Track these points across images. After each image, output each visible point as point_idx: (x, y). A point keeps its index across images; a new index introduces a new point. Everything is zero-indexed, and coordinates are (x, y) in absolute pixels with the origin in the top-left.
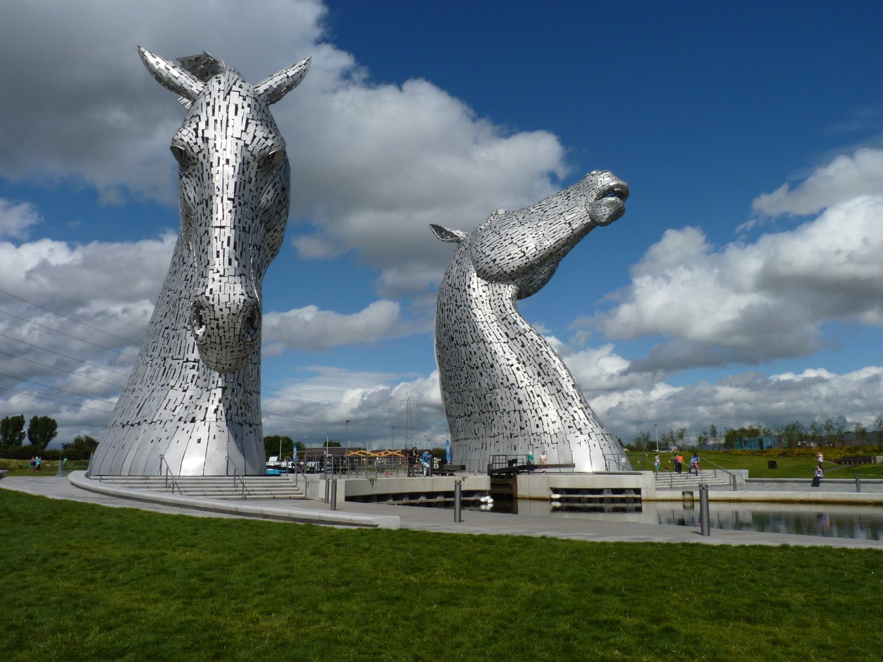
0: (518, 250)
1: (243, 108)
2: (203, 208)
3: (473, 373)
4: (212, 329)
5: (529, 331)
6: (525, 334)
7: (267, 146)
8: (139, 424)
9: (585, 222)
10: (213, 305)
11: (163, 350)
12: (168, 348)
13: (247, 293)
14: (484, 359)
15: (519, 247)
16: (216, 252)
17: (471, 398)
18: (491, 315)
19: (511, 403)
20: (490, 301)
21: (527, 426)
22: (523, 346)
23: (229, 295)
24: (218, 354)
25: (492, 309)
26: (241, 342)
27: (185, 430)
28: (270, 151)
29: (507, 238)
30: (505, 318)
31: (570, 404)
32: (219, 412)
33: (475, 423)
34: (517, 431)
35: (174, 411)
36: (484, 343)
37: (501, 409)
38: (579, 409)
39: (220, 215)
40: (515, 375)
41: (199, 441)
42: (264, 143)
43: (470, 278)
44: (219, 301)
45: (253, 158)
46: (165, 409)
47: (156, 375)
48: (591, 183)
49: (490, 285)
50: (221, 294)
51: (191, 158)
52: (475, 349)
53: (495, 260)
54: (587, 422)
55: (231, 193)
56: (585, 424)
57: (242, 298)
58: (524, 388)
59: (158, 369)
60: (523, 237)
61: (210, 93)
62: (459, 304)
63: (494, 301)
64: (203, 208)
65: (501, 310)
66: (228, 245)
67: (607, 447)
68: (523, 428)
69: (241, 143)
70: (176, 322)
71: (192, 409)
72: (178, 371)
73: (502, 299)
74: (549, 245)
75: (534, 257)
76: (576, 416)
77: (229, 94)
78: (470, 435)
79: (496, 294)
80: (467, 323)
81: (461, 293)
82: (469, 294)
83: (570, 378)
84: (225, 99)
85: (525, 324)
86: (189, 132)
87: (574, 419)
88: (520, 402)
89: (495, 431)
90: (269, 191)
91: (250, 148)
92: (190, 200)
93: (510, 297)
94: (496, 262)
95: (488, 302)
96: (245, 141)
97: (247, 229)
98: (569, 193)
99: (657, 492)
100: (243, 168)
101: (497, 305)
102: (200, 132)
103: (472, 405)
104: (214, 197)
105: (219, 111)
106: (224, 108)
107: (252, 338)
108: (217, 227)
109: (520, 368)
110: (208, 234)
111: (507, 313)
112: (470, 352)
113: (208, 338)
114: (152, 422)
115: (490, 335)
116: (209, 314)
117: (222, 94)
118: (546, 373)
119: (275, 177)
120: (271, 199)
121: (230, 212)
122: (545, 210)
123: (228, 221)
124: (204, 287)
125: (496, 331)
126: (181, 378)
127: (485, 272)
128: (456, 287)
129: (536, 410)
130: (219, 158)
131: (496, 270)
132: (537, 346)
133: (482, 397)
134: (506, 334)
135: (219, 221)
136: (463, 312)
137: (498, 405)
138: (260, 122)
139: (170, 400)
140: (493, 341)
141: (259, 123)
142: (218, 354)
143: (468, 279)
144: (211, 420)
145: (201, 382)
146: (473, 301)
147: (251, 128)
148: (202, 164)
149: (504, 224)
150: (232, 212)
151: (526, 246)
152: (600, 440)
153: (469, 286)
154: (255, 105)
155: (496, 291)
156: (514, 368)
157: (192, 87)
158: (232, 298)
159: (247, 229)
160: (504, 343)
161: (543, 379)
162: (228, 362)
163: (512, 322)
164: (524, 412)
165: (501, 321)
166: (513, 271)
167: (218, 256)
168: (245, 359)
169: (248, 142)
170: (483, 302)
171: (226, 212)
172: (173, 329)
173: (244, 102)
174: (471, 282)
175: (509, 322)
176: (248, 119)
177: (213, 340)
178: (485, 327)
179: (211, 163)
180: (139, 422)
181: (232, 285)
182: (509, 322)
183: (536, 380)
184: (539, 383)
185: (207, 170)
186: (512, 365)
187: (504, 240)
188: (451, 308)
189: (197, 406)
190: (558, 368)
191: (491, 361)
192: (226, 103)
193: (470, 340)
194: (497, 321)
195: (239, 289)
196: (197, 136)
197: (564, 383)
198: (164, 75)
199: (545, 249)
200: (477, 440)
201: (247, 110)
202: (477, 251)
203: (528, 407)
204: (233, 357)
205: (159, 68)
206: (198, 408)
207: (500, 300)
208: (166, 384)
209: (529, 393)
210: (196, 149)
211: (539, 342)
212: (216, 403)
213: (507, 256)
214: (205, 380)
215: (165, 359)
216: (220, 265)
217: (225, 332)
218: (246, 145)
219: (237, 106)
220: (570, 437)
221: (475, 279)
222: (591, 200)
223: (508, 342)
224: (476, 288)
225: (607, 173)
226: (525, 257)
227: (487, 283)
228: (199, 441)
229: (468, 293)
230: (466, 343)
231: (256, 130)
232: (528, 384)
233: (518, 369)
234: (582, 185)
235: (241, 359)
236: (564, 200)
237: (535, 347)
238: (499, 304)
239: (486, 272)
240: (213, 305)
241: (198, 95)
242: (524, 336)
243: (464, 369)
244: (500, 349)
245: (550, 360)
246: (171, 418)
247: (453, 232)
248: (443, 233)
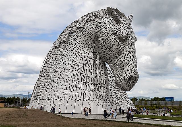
2: (128, 53)
8: (86, 100)
11: (83, 80)
12: (85, 79)
31: (124, 95)
35: (97, 97)
59: (83, 85)
64: (128, 53)
70: (86, 72)
72: (92, 87)
87: (126, 99)
110: (133, 60)
114: (92, 100)
148: (128, 43)
164: (113, 96)
172: (85, 74)
179: (131, 43)
185: (130, 45)
208: (89, 90)
210: (127, 39)
214: (102, 90)
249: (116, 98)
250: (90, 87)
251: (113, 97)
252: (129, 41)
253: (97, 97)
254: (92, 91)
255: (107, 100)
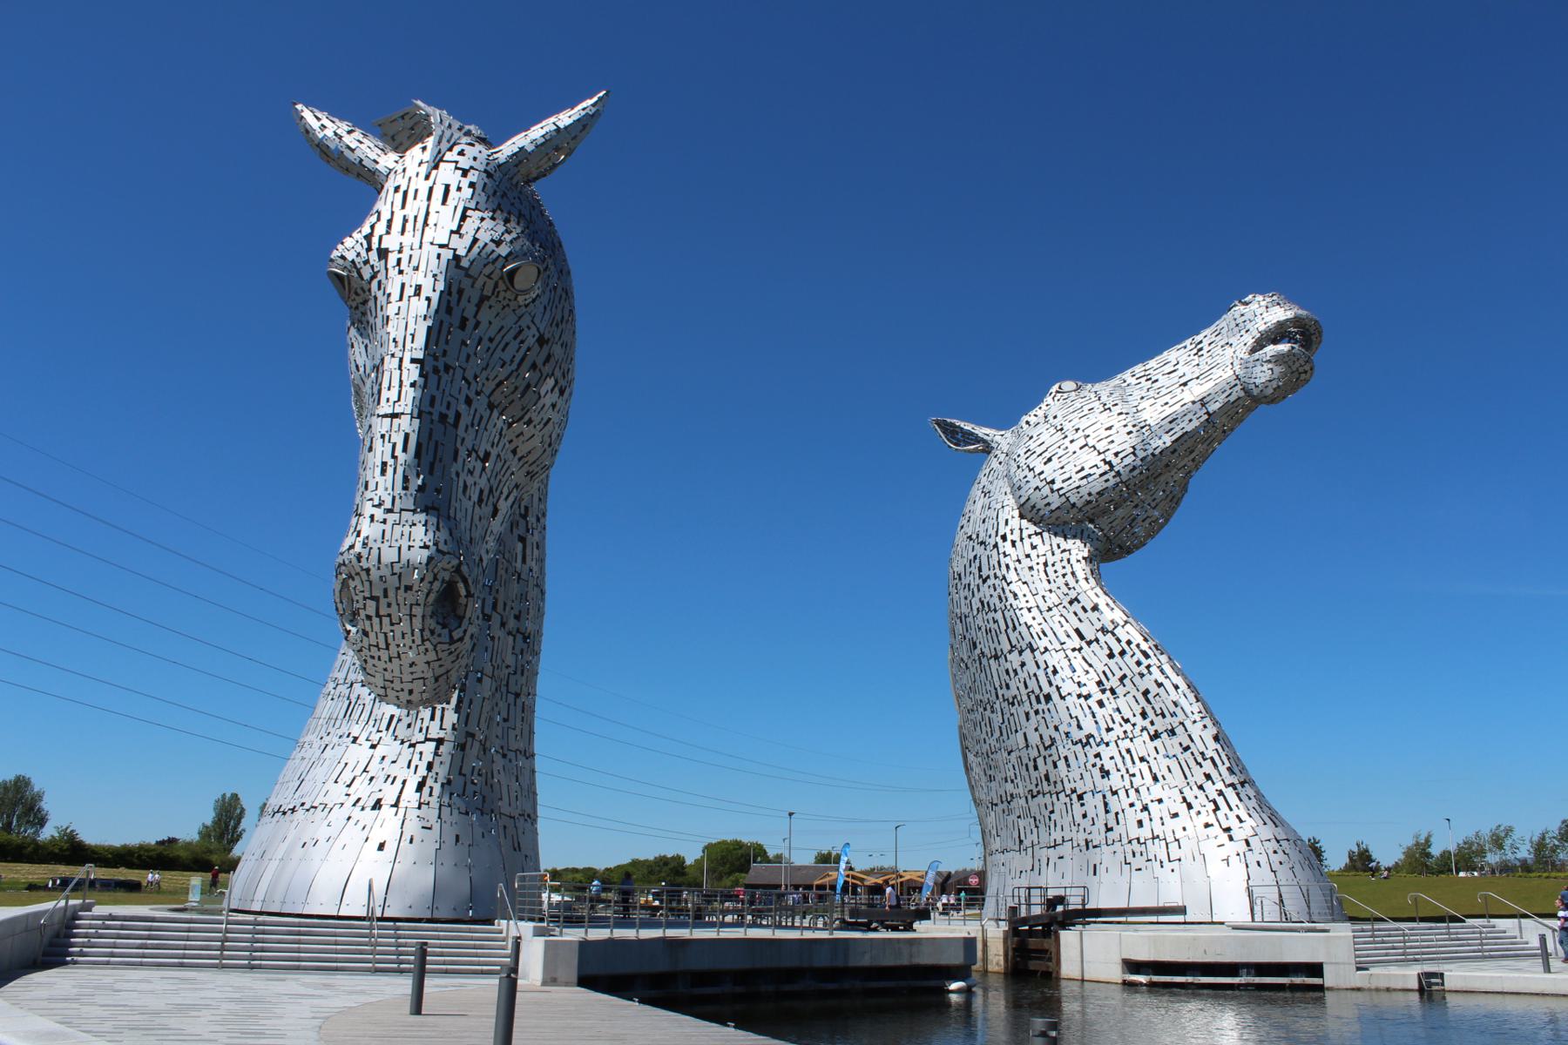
0: (1097, 460)
1: (459, 189)
3: (1012, 715)
4: (369, 618)
5: (1122, 623)
6: (1115, 631)
7: (500, 255)
8: (293, 810)
9: (1232, 398)
10: (368, 570)
11: (352, 667)
13: (436, 544)
14: (1032, 684)
15: (1100, 453)
16: (380, 464)
17: (1010, 766)
18: (1047, 594)
19: (1087, 776)
20: (1046, 564)
21: (1118, 823)
22: (1111, 656)
23: (400, 548)
24: (385, 670)
25: (1049, 582)
26: (428, 644)
27: (360, 825)
28: (504, 267)
29: (1076, 437)
30: (1076, 599)
31: (1208, 777)
32: (426, 790)
33: (1019, 817)
34: (1097, 838)
35: (349, 786)
36: (1033, 651)
37: (1068, 787)
38: (1227, 786)
39: (393, 395)
40: (1094, 717)
41: (381, 847)
42: (493, 251)
43: (1007, 521)
44: (379, 562)
45: (470, 281)
46: (336, 782)
47: (335, 717)
48: (1243, 318)
49: (1046, 535)
50: (385, 547)
51: (359, 291)
52: (1016, 665)
53: (1053, 482)
54: (1244, 816)
55: (417, 348)
56: (1238, 817)
57: (426, 553)
58: (1112, 745)
60: (1109, 432)
61: (404, 170)
62: (985, 573)
63: (1053, 565)
65: (1067, 585)
66: (405, 450)
67: (1286, 867)
68: (1111, 829)
69: (447, 255)
71: (378, 783)
72: (368, 708)
73: (1069, 560)
74: (1164, 446)
75: (1131, 471)
76: (1220, 801)
77: (436, 167)
78: (1010, 845)
79: (1057, 551)
80: (1000, 612)
81: (988, 552)
82: (1004, 553)
83: (1207, 721)
84: (427, 177)
85: (1116, 609)
86: (357, 242)
87: (1217, 808)
88: (1105, 773)
89: (1057, 835)
90: (507, 344)
91: (465, 263)
92: (358, 370)
93: (1086, 555)
94: (1055, 487)
95: (1041, 567)
96: (455, 250)
97: (451, 420)
98: (1201, 342)
99: (1358, 972)
100: (449, 302)
101: (1059, 574)
102: (375, 240)
103: (1012, 781)
104: (387, 359)
105: (415, 198)
106: (423, 194)
107: (451, 637)
108: (385, 416)
109: (1106, 702)
111: (1079, 590)
112: (1007, 672)
113: (365, 638)
115: (1045, 635)
116: (362, 589)
117: (425, 166)
118: (1159, 712)
119: (520, 318)
120: (512, 361)
121: (413, 385)
122: (1154, 379)
123: (407, 405)
124: (356, 533)
125: (1056, 627)
126: (371, 722)
127: (1034, 507)
128: (980, 540)
129: (1137, 791)
130: (403, 285)
131: (1056, 501)
132: (1139, 656)
133: (1031, 765)
134: (1077, 631)
135: (391, 403)
136: (992, 589)
137: (1062, 781)
138: (491, 214)
139: (346, 764)
140: (1050, 647)
141: (487, 215)
142: (385, 670)
143: (1002, 523)
144: (409, 805)
145: (402, 731)
146: (1012, 566)
147: (470, 227)
148: (376, 298)
149: (1071, 409)
150: (418, 384)
151: (1115, 451)
152: (1270, 852)
153: (1004, 538)
154: (485, 184)
155: (1059, 547)
156: (1092, 702)
157: (377, 163)
158: (405, 555)
159: (451, 420)
160: (1074, 650)
161: (1152, 723)
162: (410, 686)
163: (1088, 608)
164: (1115, 793)
165: (1068, 606)
166: (1089, 502)
167: (383, 472)
168: (440, 679)
169: (462, 252)
170: (1031, 568)
171: (407, 383)
173: (463, 179)
174: (1009, 528)
175: (1083, 608)
176: (465, 209)
177: (373, 641)
178: (1034, 618)
179: (389, 295)
180: (295, 807)
181: (407, 529)
182: (1083, 608)
183: (1138, 728)
184: (1145, 733)
186: (1087, 697)
187: (1072, 442)
188: (972, 583)
189: (389, 776)
190: (1183, 701)
191: (1046, 689)
192: (429, 183)
193: (1007, 647)
194: (1060, 607)
195: (419, 533)
196: (369, 249)
197: (1195, 731)
198: (332, 146)
199: (1153, 454)
200: (1023, 853)
201: (467, 192)
202: (1019, 467)
203: (1121, 784)
204: (415, 676)
205: (325, 135)
206: (390, 780)
207: (1065, 563)
209: (1124, 753)
210: (367, 273)
211: (1144, 646)
212: (422, 771)
213: (1077, 473)
215: (352, 684)
216: (386, 489)
217: (392, 624)
218: (457, 258)
219: (447, 187)
220: (1209, 848)
221: (1015, 523)
222: (1242, 353)
223: (1081, 649)
224: (1018, 540)
225: (1275, 298)
226: (1113, 473)
227: (1039, 530)
228: (381, 847)
229: (1001, 551)
230: (999, 653)
231: (479, 228)
232: (1122, 736)
233: (1101, 704)
234: (1224, 324)
235: (433, 680)
236: (1192, 357)
237: (1135, 658)
238: (1064, 571)
239: (1038, 507)
240: (368, 570)
241: (387, 176)
242: (1114, 634)
243: (997, 706)
244: (1065, 663)
245: (1167, 683)
246: (343, 799)
247: (976, 432)
248: (959, 436)
249: (1132, 805)
250: (361, 707)
251: (1111, 799)
252: (380, 282)
253: (349, 786)
254: (355, 740)
255: (396, 805)
